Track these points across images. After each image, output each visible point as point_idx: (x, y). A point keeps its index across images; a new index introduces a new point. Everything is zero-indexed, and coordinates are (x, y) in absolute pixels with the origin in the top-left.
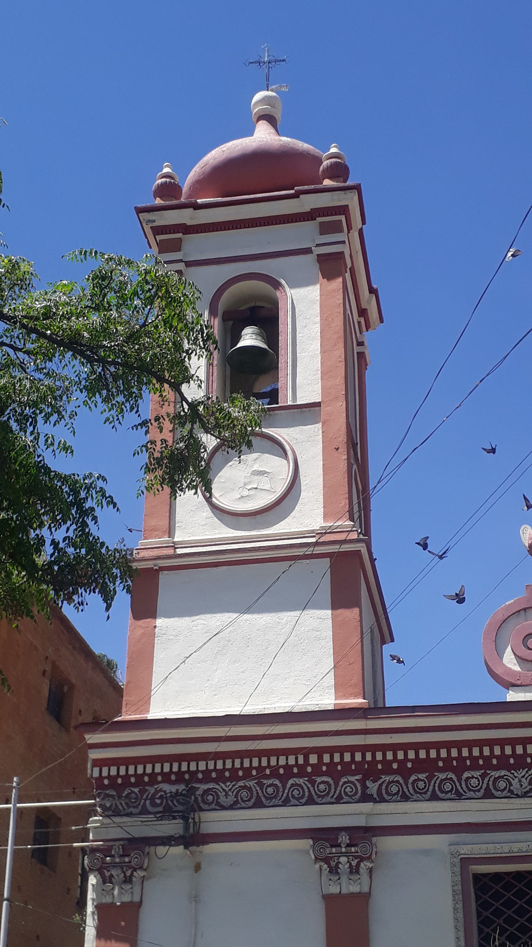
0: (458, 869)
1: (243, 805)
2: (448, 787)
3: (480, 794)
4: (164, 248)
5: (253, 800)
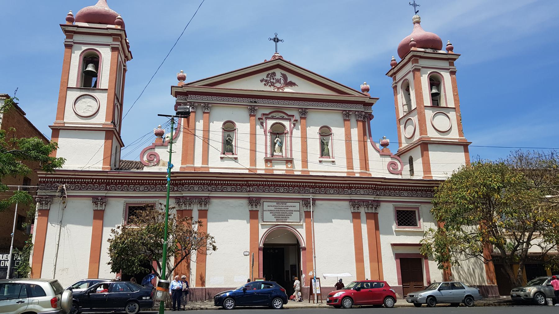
0: (125, 205)
1: (77, 189)
2: (126, 188)
3: (132, 190)
5: (79, 188)
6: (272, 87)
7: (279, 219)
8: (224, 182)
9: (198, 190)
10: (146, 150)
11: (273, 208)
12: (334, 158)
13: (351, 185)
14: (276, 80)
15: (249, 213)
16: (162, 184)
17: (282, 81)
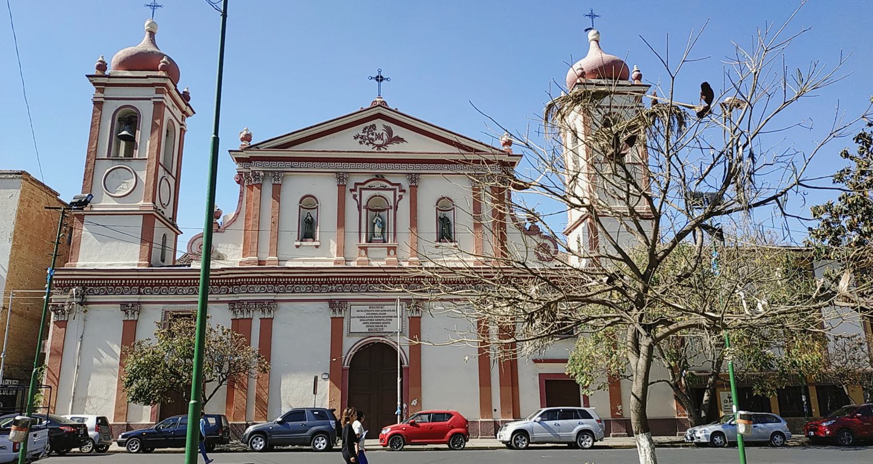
0: (164, 314)
2: (164, 291)
4: (98, 90)
6: (371, 145)
7: (372, 328)
8: (296, 280)
10: (194, 239)
11: (364, 314)
14: (376, 135)
16: (213, 285)
17: (385, 137)
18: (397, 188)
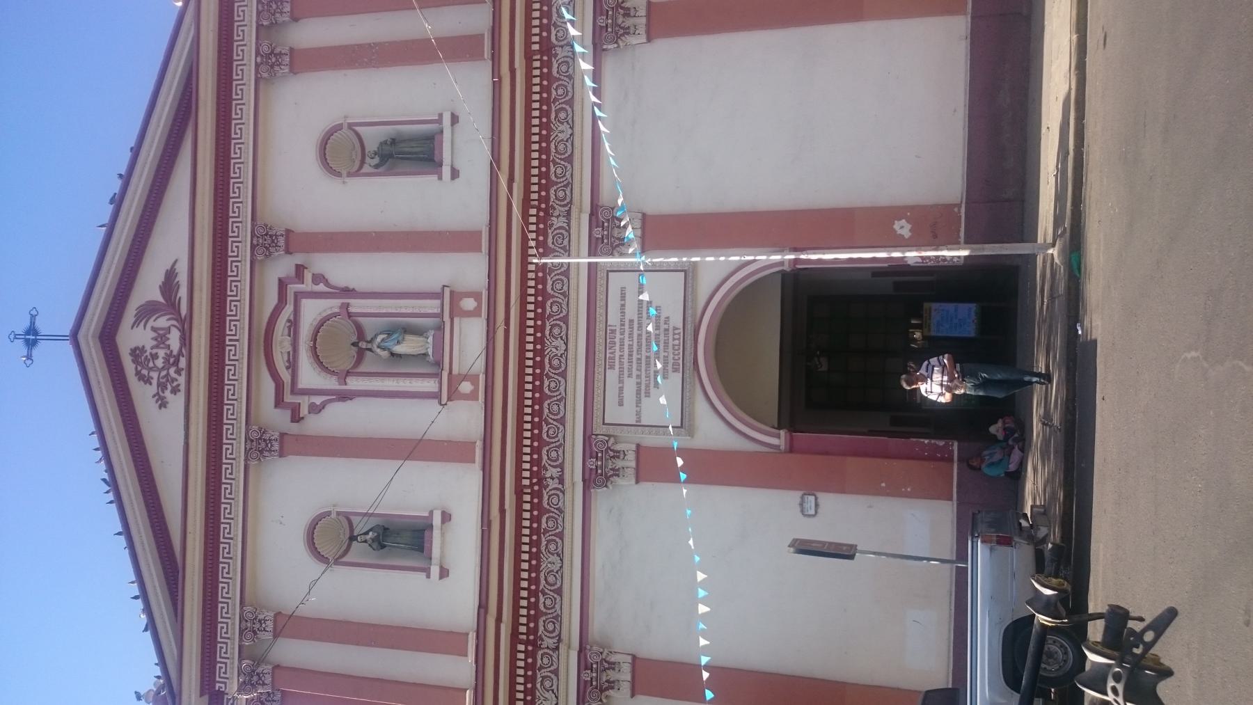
6: (183, 363)
8: (524, 584)
9: (553, 691)
11: (630, 386)
12: (441, 115)
13: (536, 47)
14: (157, 347)
15: (646, 486)
17: (163, 322)
18: (293, 288)
